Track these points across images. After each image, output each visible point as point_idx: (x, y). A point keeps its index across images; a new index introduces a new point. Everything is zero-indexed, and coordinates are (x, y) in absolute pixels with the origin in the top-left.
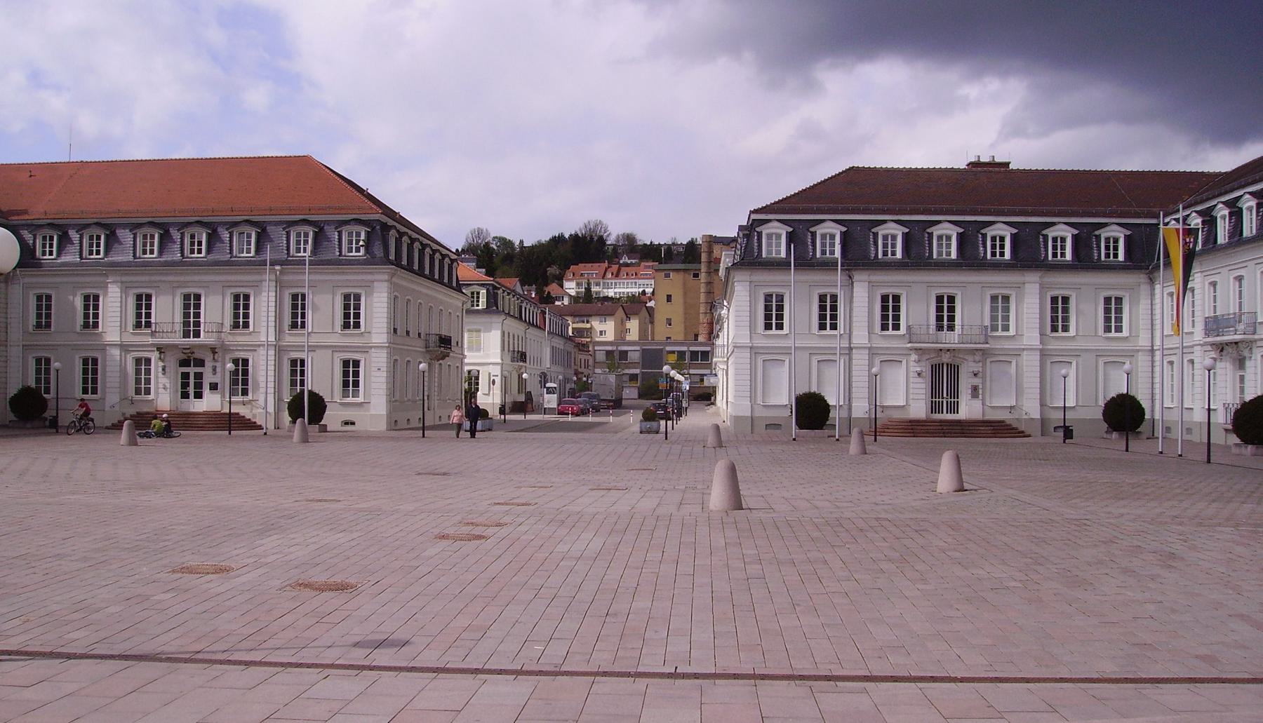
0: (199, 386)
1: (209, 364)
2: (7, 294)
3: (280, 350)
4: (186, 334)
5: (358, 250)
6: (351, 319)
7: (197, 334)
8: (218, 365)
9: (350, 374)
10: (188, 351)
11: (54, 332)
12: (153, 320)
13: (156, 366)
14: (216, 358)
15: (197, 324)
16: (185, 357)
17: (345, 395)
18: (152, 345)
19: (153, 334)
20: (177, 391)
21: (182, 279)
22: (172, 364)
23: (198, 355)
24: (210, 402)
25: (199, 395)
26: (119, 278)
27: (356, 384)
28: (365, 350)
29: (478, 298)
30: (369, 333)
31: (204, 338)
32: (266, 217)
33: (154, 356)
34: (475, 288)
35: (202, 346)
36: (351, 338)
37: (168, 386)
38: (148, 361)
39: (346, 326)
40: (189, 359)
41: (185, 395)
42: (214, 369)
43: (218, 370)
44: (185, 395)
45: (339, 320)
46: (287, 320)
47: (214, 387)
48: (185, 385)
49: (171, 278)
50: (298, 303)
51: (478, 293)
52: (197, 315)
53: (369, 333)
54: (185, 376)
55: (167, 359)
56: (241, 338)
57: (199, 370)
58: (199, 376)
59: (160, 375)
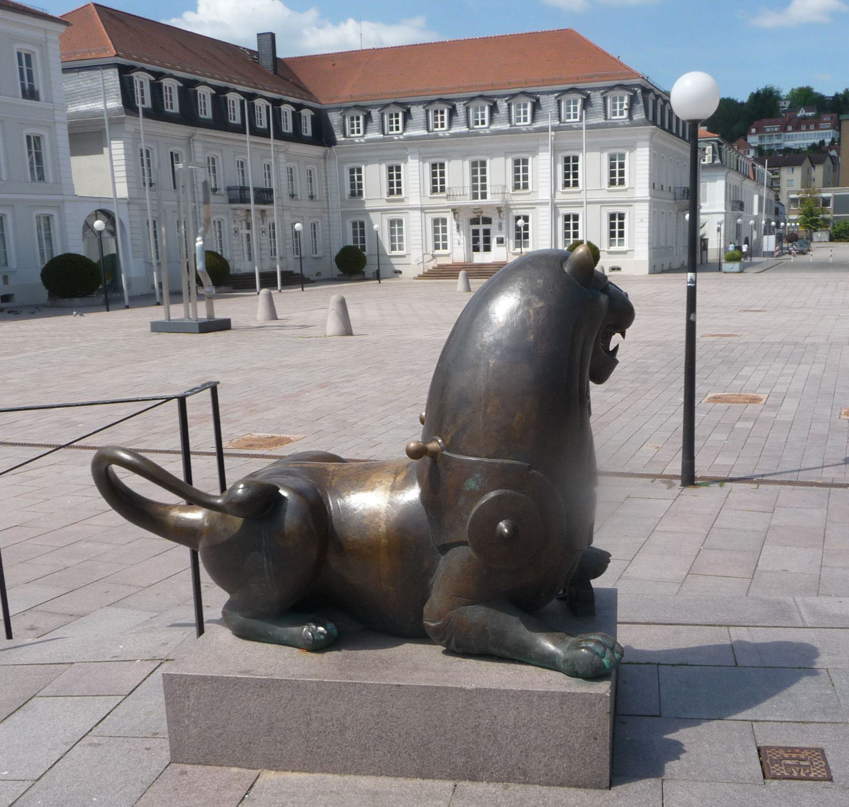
0: (487, 240)
1: (495, 222)
2: (325, 169)
4: (475, 196)
5: (621, 113)
6: (616, 176)
7: (484, 196)
8: (504, 222)
10: (478, 211)
11: (366, 199)
12: (447, 185)
13: (451, 224)
14: (501, 216)
15: (484, 187)
16: (475, 216)
17: (611, 243)
18: (447, 207)
20: (469, 245)
22: (465, 223)
23: (485, 215)
25: (487, 249)
27: (621, 234)
28: (629, 203)
32: (540, 87)
33: (449, 217)
36: (617, 193)
37: (462, 241)
38: (444, 221)
39: (612, 183)
41: (476, 249)
42: (500, 226)
43: (504, 226)
47: (500, 241)
48: (476, 240)
52: (484, 179)
54: (476, 232)
55: (460, 218)
56: (519, 199)
57: (487, 227)
58: (487, 232)
59: (455, 232)
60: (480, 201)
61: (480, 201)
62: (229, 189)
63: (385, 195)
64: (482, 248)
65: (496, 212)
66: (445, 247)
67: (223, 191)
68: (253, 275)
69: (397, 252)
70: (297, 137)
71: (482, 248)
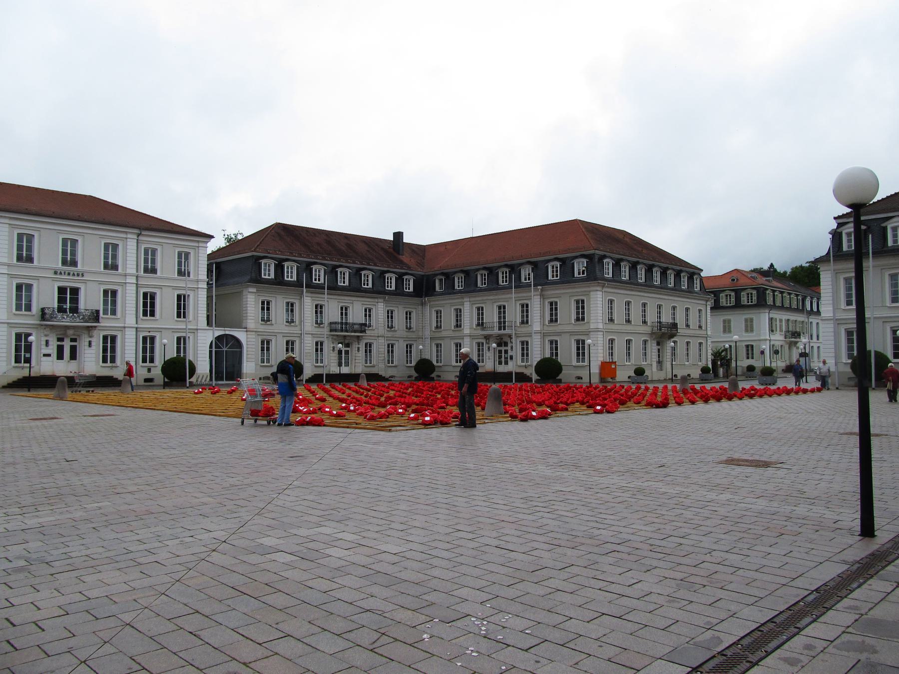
0: (506, 358)
1: (509, 345)
3: (544, 335)
4: (500, 329)
5: (583, 274)
9: (581, 349)
11: (443, 330)
13: (485, 347)
17: (578, 361)
19: (483, 329)
21: (496, 297)
24: (511, 367)
25: (506, 363)
26: (468, 299)
29: (752, 297)
30: (588, 323)
31: (507, 331)
34: (749, 291)
35: (505, 335)
36: (580, 327)
38: (483, 344)
40: (502, 342)
44: (500, 363)
45: (574, 316)
46: (548, 318)
49: (491, 297)
50: (553, 306)
51: (751, 294)
52: (504, 317)
53: (588, 323)
54: (500, 352)
56: (524, 329)
58: (506, 352)
60: (502, 332)
61: (502, 332)
62: (331, 323)
63: (453, 328)
64: (503, 363)
65: (509, 339)
66: (483, 362)
67: (326, 324)
68: (323, 375)
69: (439, 364)
70: (399, 292)
71: (503, 363)
